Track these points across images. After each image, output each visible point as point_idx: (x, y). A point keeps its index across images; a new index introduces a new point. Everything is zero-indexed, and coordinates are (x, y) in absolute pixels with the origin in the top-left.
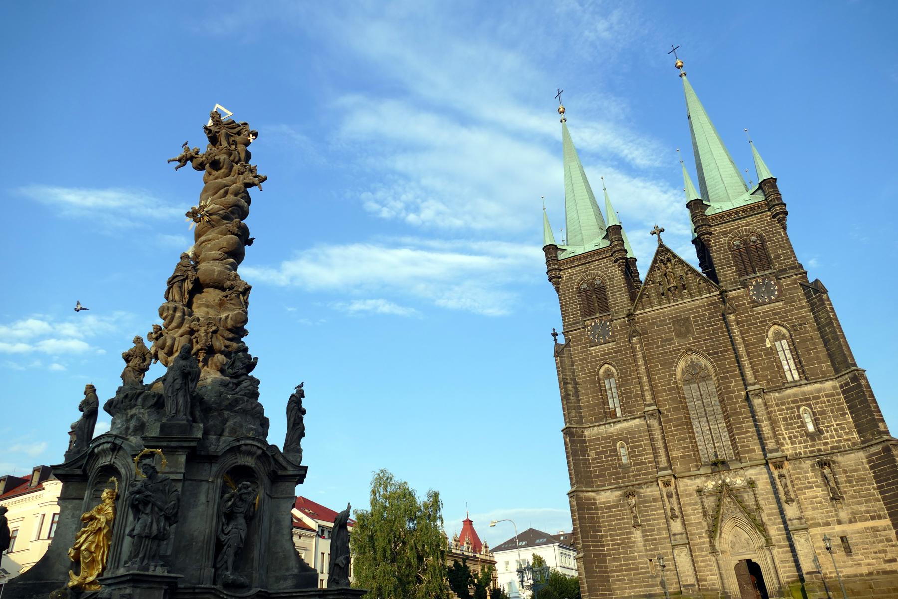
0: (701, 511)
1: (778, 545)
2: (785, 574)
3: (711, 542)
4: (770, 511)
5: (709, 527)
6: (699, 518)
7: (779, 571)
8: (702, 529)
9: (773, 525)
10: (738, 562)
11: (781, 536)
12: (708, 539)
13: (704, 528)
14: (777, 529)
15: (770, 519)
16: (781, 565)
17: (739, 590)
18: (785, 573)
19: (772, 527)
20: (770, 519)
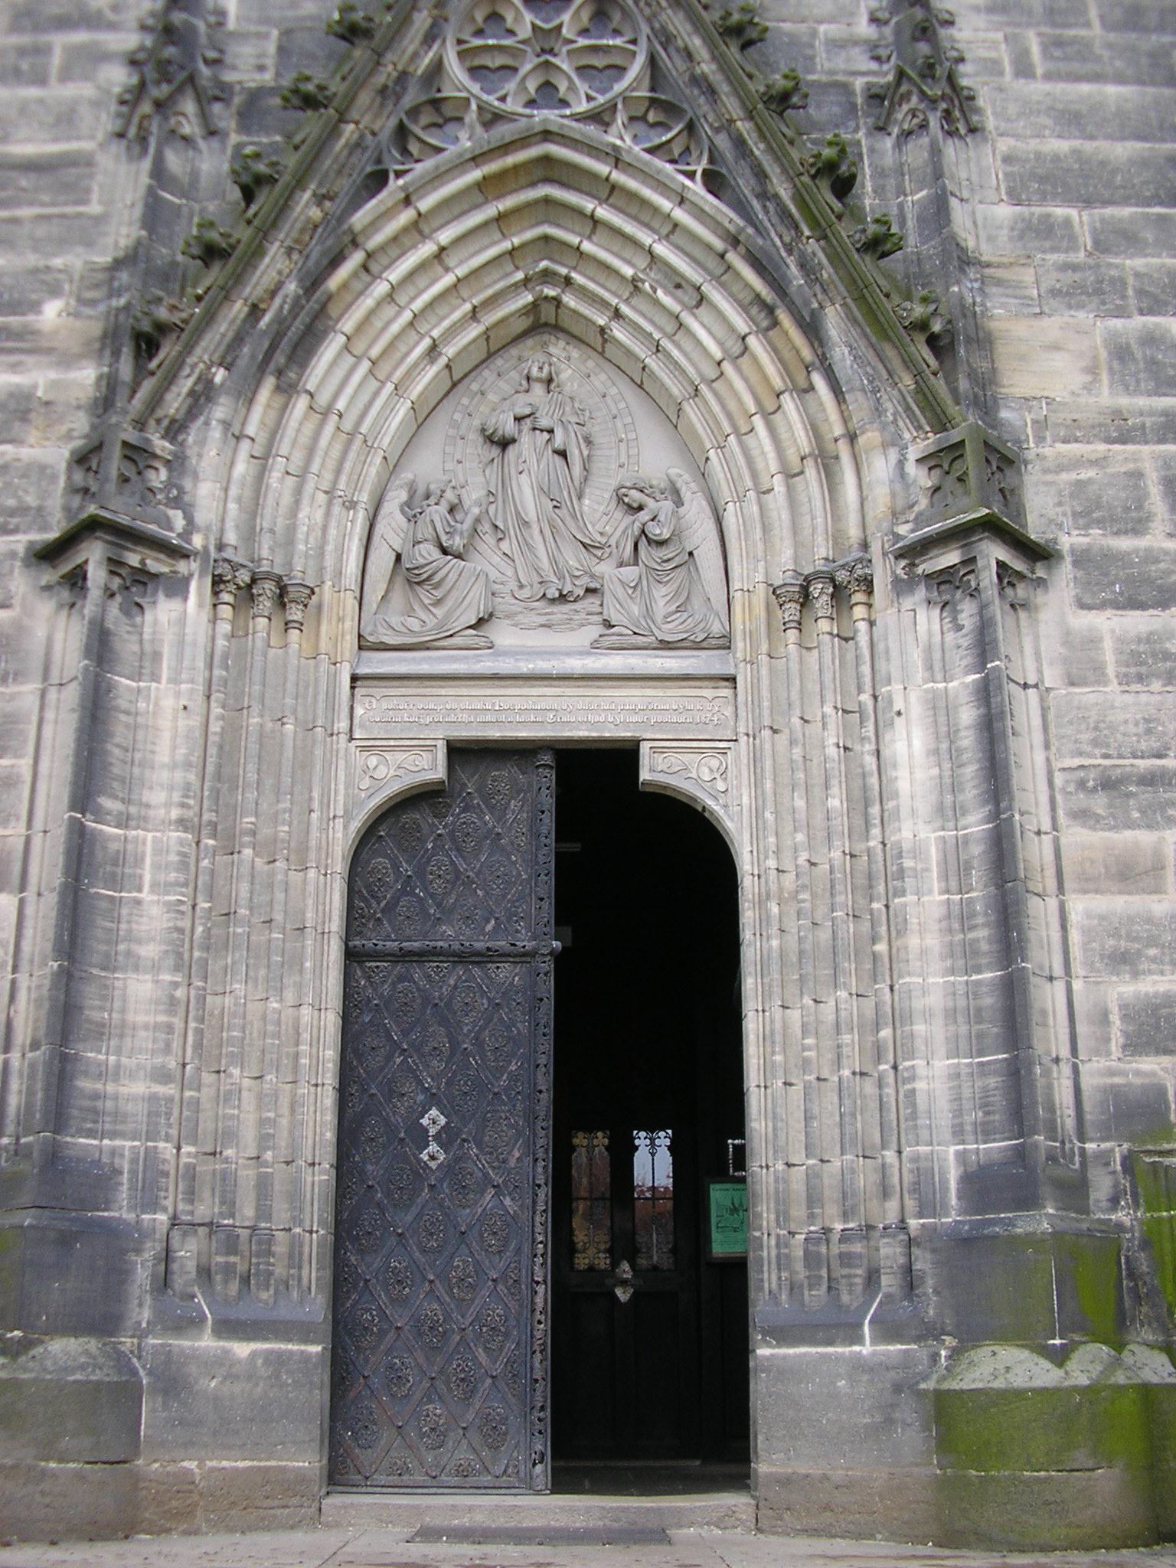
0: (130, 40)
1: (1082, 559)
2: (1124, 989)
3: (105, 401)
4: (1062, 146)
5: (154, 214)
6: (65, 120)
7: (1041, 913)
8: (62, 244)
9: (1070, 295)
10: (432, 768)
11: (1147, 456)
12: (86, 376)
13: (86, 231)
14: (1121, 353)
15: (1045, 231)
16: (1076, 837)
17: (320, 1178)
18: (1123, 961)
19: (1052, 326)
20: (1045, 231)
